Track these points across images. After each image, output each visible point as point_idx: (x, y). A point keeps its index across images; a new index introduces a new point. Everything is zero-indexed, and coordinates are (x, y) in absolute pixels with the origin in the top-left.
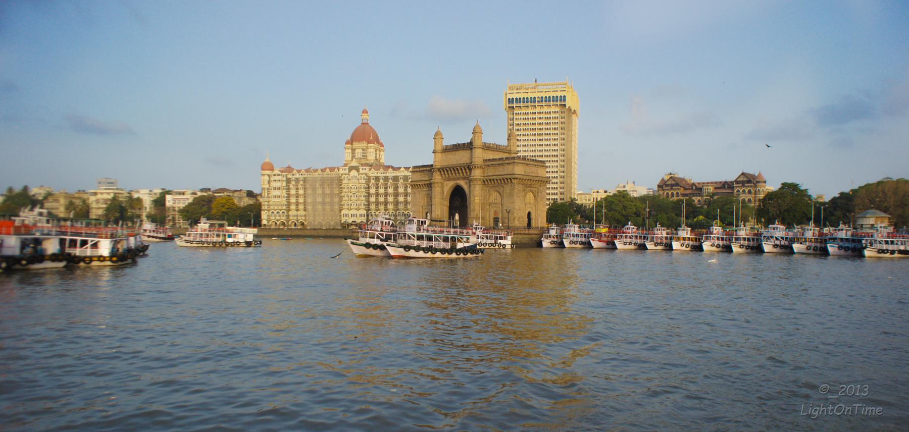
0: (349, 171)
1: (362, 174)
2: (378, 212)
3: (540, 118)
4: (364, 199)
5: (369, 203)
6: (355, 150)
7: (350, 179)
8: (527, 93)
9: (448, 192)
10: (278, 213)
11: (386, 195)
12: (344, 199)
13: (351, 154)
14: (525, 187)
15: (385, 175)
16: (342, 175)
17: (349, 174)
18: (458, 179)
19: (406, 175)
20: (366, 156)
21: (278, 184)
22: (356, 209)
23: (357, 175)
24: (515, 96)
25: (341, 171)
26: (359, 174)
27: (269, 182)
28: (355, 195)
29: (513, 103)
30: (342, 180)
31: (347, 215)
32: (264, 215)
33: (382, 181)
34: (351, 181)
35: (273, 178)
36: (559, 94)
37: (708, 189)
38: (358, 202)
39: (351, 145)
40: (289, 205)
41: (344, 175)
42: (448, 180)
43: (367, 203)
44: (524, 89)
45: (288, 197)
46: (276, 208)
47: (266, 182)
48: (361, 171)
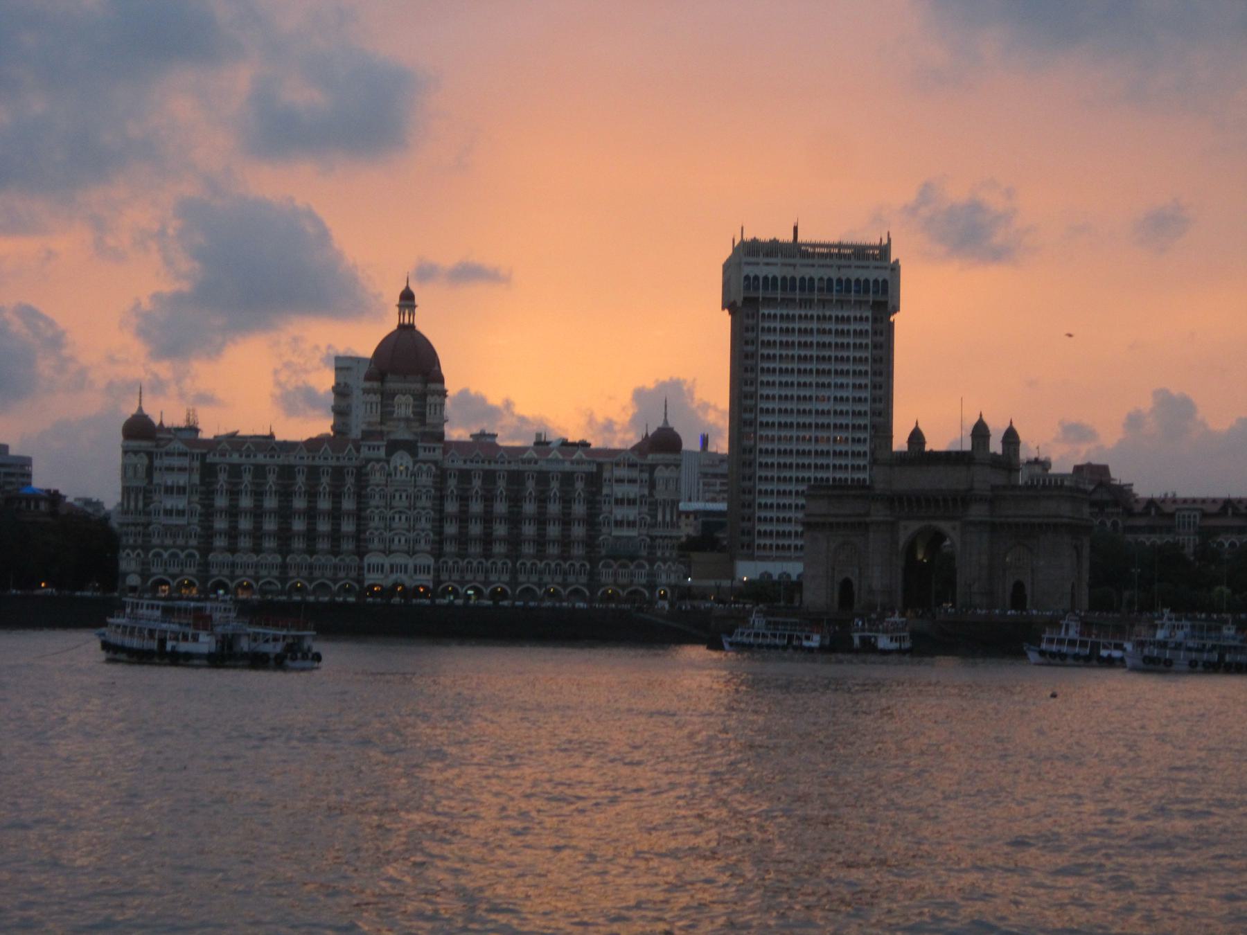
1: (425, 462)
2: (466, 561)
3: (824, 332)
4: (429, 526)
5: (440, 540)
6: (393, 395)
7: (389, 475)
8: (794, 266)
10: (174, 555)
11: (488, 519)
12: (372, 525)
15: (486, 466)
16: (368, 461)
19: (544, 468)
21: (182, 480)
22: (408, 553)
23: (411, 465)
24: (762, 271)
25: (365, 453)
27: (150, 471)
28: (403, 517)
29: (756, 288)
30: (367, 475)
31: (381, 568)
32: (128, 563)
33: (477, 483)
35: (167, 461)
36: (872, 275)
37: (1189, 517)
38: (412, 535)
40: (208, 535)
43: (437, 538)
45: (208, 513)
46: (168, 542)
47: (142, 471)
48: (422, 455)
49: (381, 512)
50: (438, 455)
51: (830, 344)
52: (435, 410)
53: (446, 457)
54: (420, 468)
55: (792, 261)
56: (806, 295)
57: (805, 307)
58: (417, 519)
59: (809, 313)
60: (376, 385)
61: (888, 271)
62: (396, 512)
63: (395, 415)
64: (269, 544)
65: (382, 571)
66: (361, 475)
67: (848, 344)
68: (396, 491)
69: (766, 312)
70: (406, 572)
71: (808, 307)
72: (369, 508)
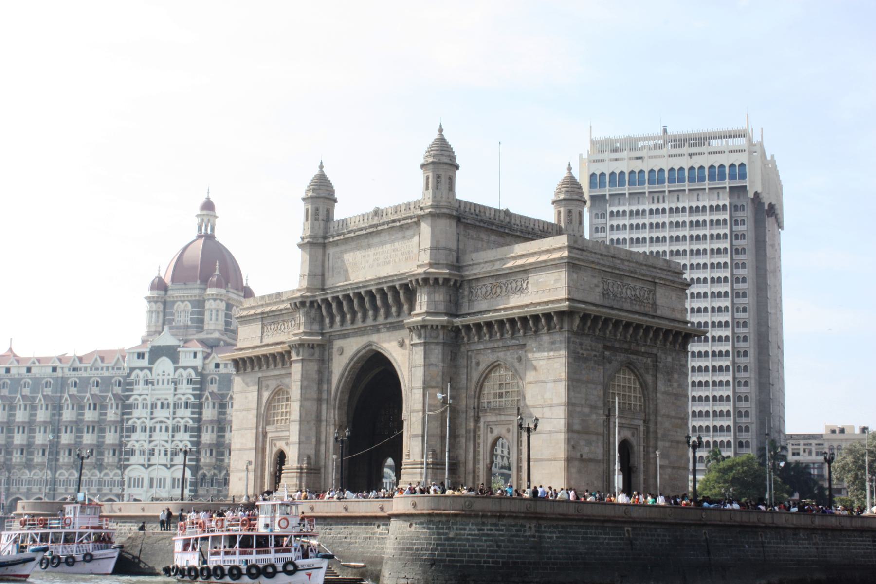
0: (152, 361)
1: (185, 368)
9: (342, 375)
13: (161, 315)
14: (606, 348)
16: (132, 369)
17: (150, 369)
18: (376, 329)
20: (202, 321)
24: (607, 168)
26: (176, 369)
28: (164, 429)
30: (131, 384)
31: (138, 483)
34: (156, 387)
36: (726, 160)
39: (162, 293)
41: (137, 371)
42: (344, 336)
44: (631, 150)
48: (183, 361)
49: (143, 422)
50: (198, 362)
51: (684, 237)
52: (217, 315)
53: (207, 361)
54: (181, 375)
55: (639, 154)
56: (657, 188)
57: (658, 202)
58: (176, 429)
59: (661, 206)
60: (155, 293)
61: (746, 155)
62: (157, 423)
63: (174, 324)
64: (38, 458)
65: (142, 487)
66: (127, 384)
67: (705, 236)
68: (158, 399)
69: (615, 209)
70: (164, 487)
71: (661, 200)
72: (131, 418)
